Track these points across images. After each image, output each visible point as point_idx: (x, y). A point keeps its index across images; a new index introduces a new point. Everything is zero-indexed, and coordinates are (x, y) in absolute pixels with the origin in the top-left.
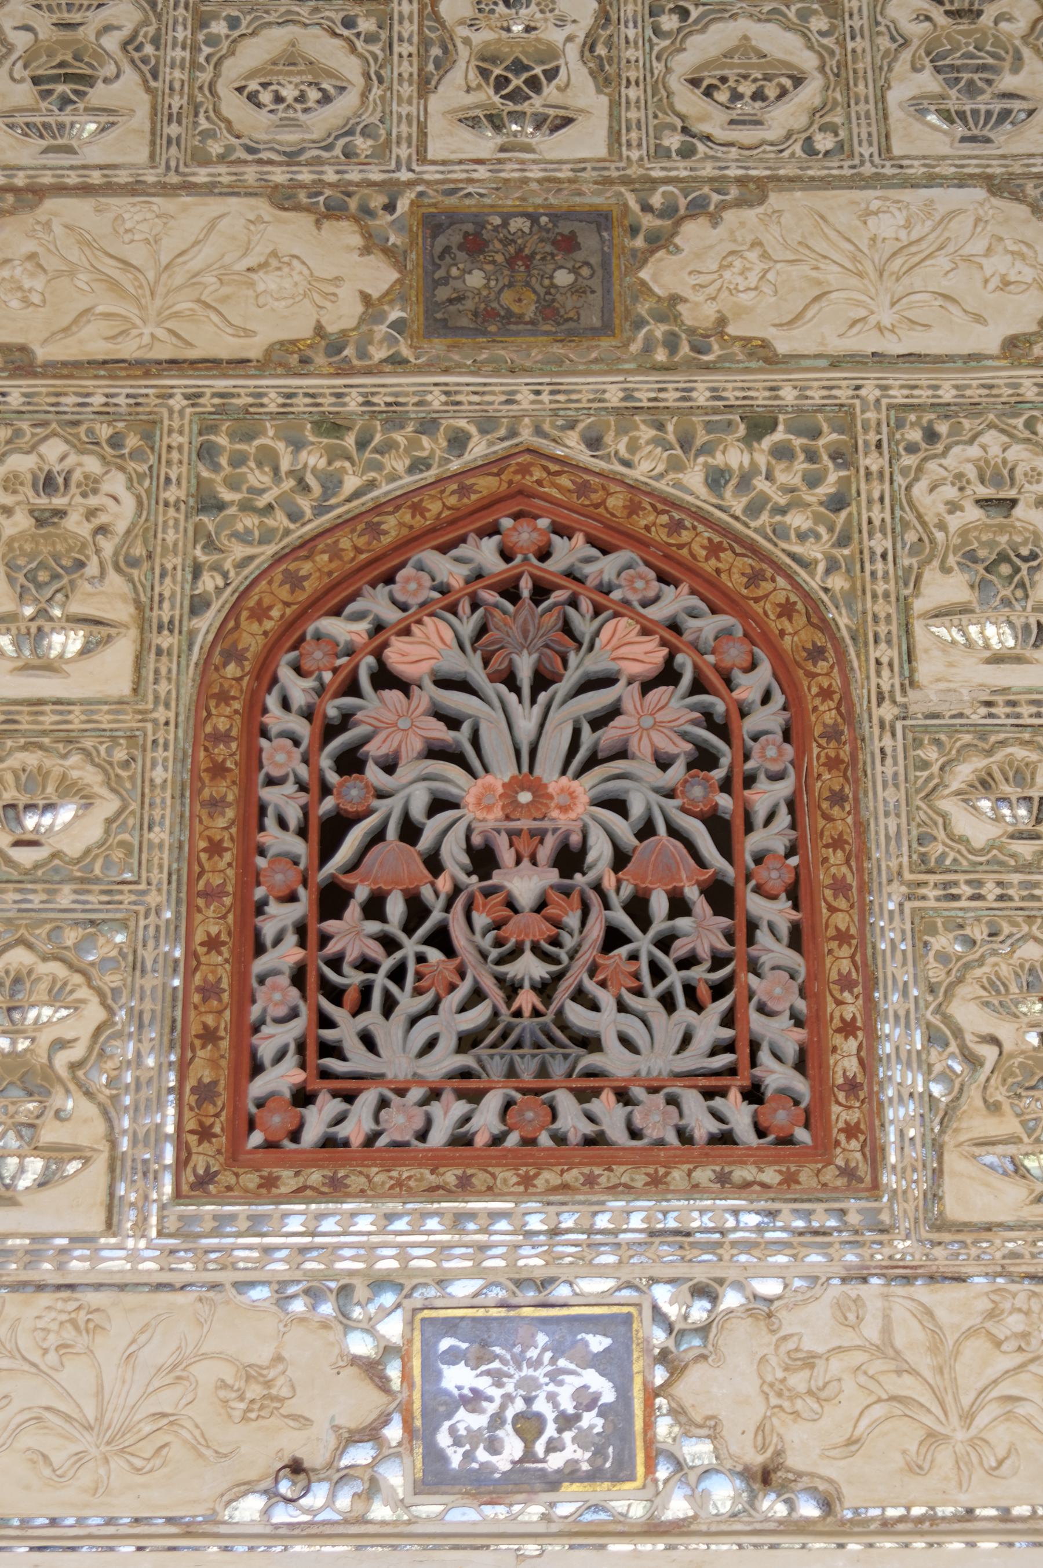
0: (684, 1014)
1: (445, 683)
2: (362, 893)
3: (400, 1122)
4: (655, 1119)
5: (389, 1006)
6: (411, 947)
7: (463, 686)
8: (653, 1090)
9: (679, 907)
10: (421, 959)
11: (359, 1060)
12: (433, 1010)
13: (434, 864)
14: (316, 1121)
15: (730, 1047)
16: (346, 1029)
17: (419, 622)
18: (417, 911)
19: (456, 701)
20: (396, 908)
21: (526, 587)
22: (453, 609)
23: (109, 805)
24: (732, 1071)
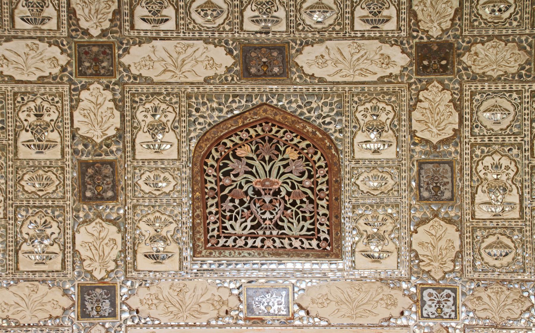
0: (302, 223)
1: (248, 158)
2: (229, 198)
3: (240, 242)
4: (296, 244)
5: (236, 220)
6: (240, 208)
7: (252, 159)
8: (296, 238)
9: (302, 202)
10: (243, 211)
11: (230, 230)
12: (246, 221)
13: (246, 193)
14: (222, 241)
15: (313, 230)
16: (227, 224)
17: (244, 145)
18: (242, 203)
19: (250, 162)
20: (237, 201)
21: (267, 138)
22: (251, 142)
23: (174, 183)
24: (313, 235)
